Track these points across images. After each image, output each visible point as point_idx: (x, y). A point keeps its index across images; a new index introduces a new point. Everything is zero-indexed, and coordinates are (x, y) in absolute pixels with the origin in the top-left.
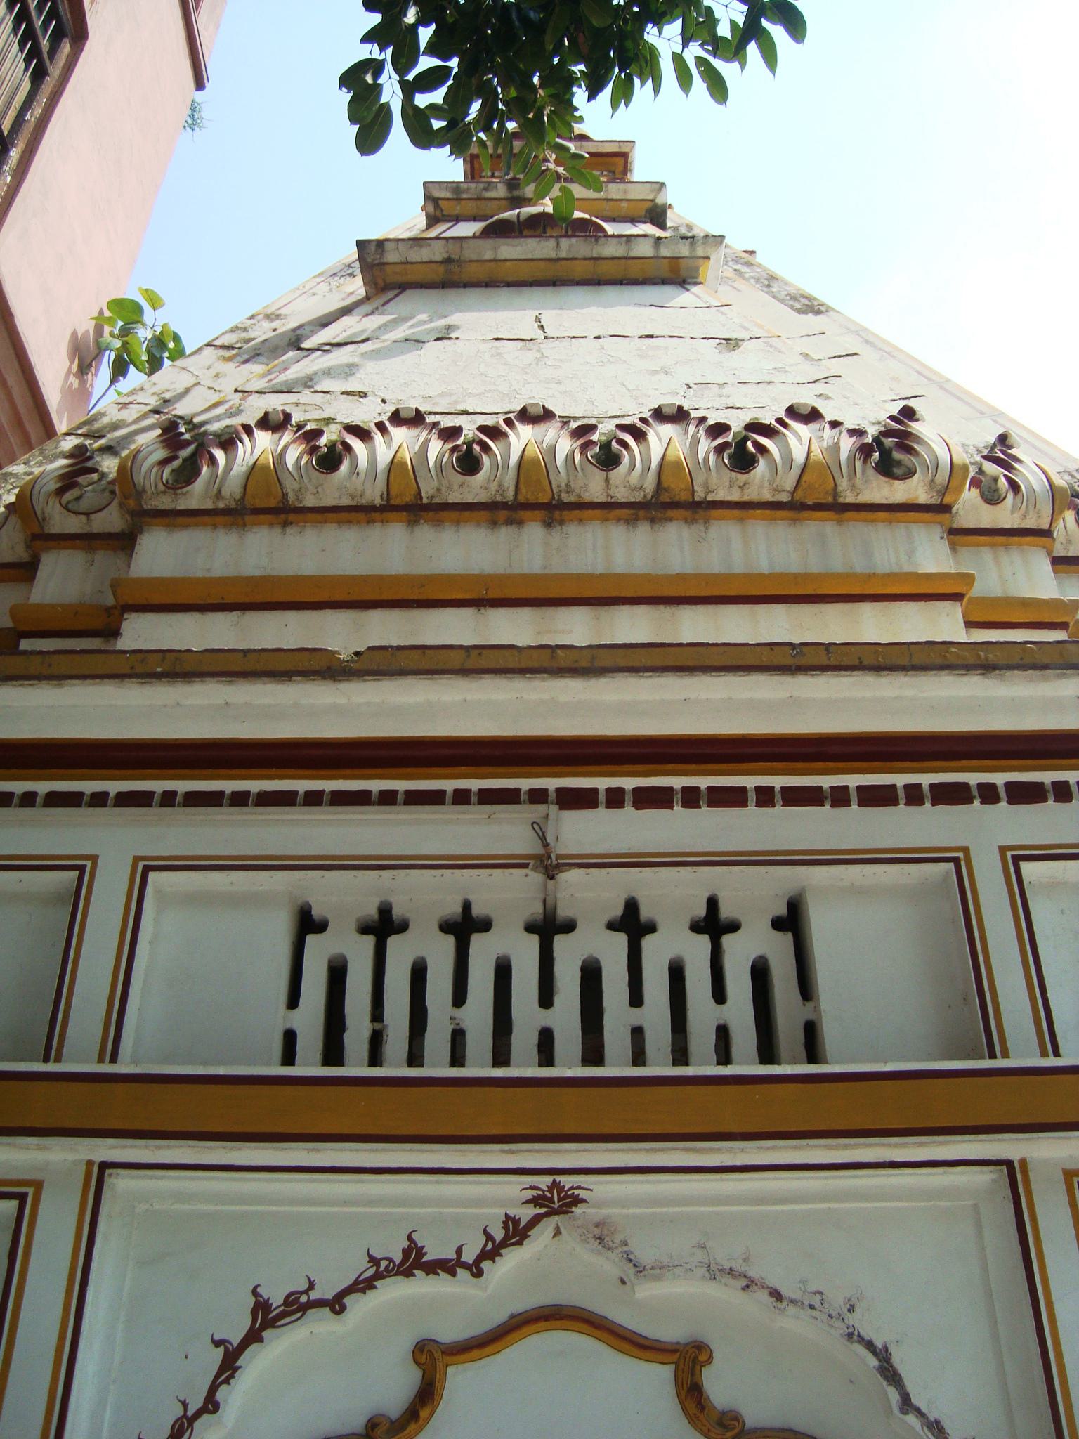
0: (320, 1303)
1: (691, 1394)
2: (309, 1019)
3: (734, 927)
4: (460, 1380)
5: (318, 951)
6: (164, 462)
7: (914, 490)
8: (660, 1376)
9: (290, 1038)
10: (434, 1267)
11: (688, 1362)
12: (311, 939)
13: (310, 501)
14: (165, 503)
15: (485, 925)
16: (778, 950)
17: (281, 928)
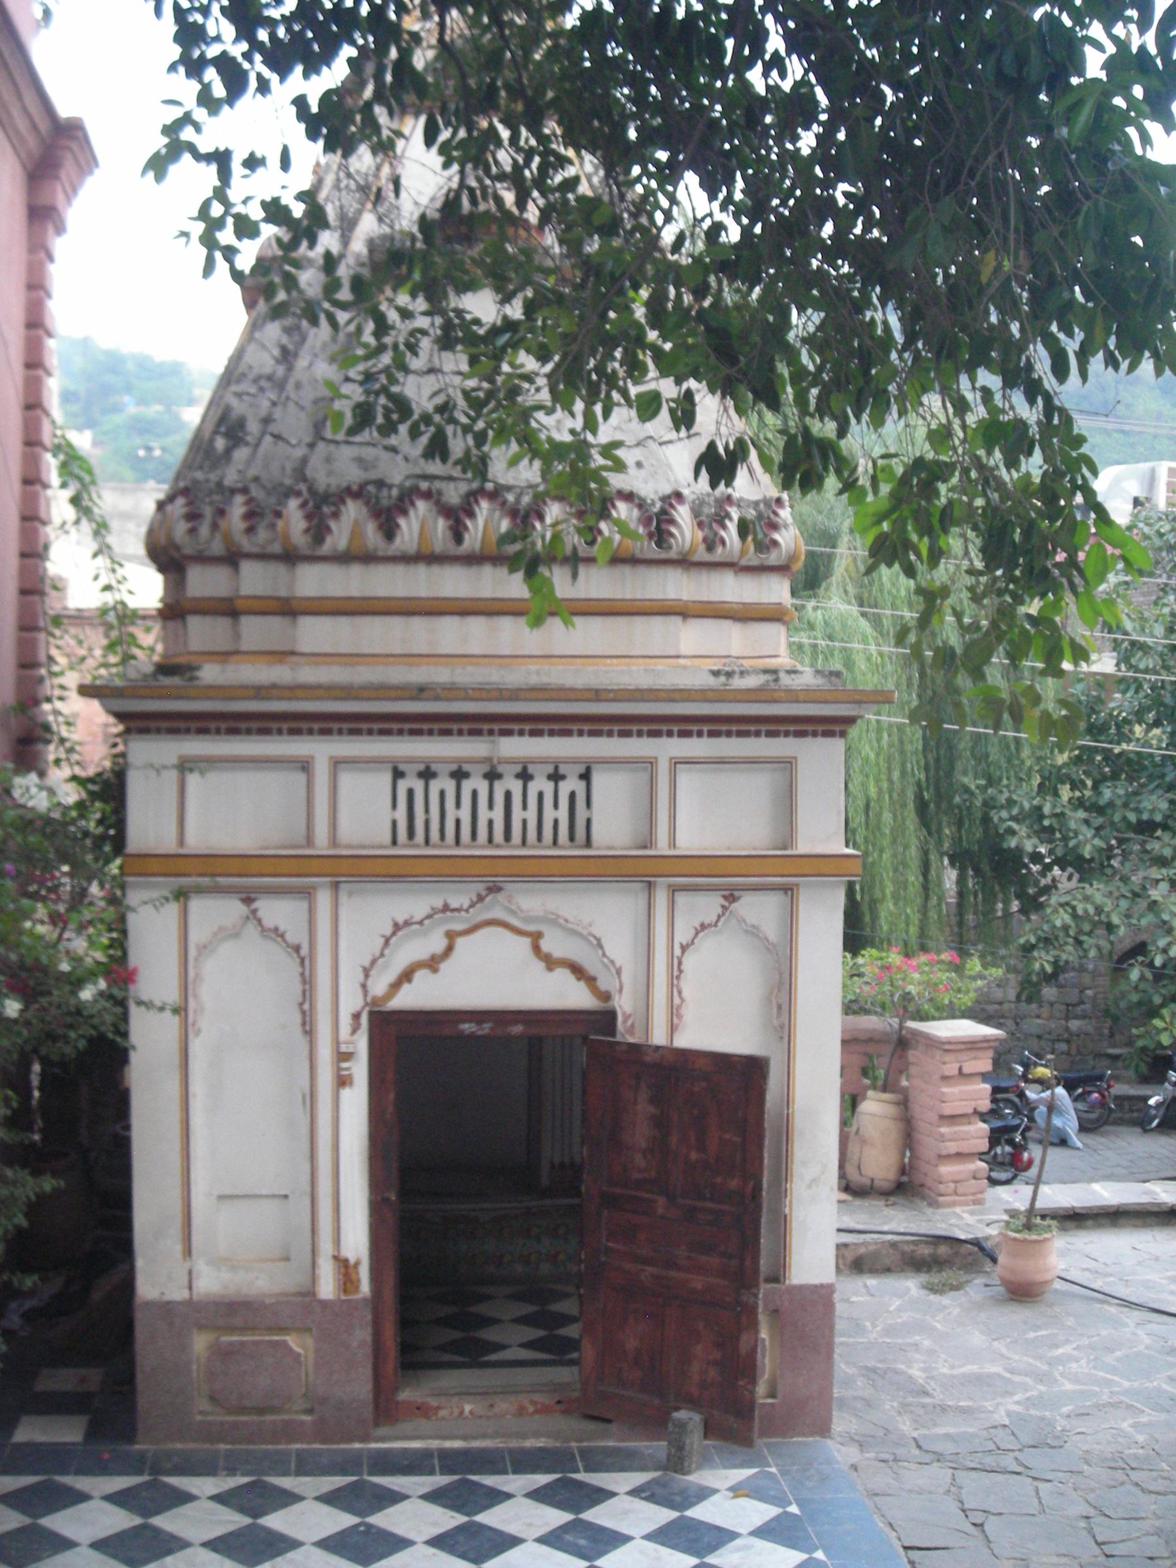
1: (536, 949)
3: (563, 777)
4: (460, 942)
5: (403, 786)
6: (307, 531)
7: (673, 554)
8: (527, 941)
9: (394, 824)
10: (454, 910)
11: (536, 937)
13: (380, 553)
14: (307, 552)
15: (466, 775)
16: (579, 787)
17: (387, 778)
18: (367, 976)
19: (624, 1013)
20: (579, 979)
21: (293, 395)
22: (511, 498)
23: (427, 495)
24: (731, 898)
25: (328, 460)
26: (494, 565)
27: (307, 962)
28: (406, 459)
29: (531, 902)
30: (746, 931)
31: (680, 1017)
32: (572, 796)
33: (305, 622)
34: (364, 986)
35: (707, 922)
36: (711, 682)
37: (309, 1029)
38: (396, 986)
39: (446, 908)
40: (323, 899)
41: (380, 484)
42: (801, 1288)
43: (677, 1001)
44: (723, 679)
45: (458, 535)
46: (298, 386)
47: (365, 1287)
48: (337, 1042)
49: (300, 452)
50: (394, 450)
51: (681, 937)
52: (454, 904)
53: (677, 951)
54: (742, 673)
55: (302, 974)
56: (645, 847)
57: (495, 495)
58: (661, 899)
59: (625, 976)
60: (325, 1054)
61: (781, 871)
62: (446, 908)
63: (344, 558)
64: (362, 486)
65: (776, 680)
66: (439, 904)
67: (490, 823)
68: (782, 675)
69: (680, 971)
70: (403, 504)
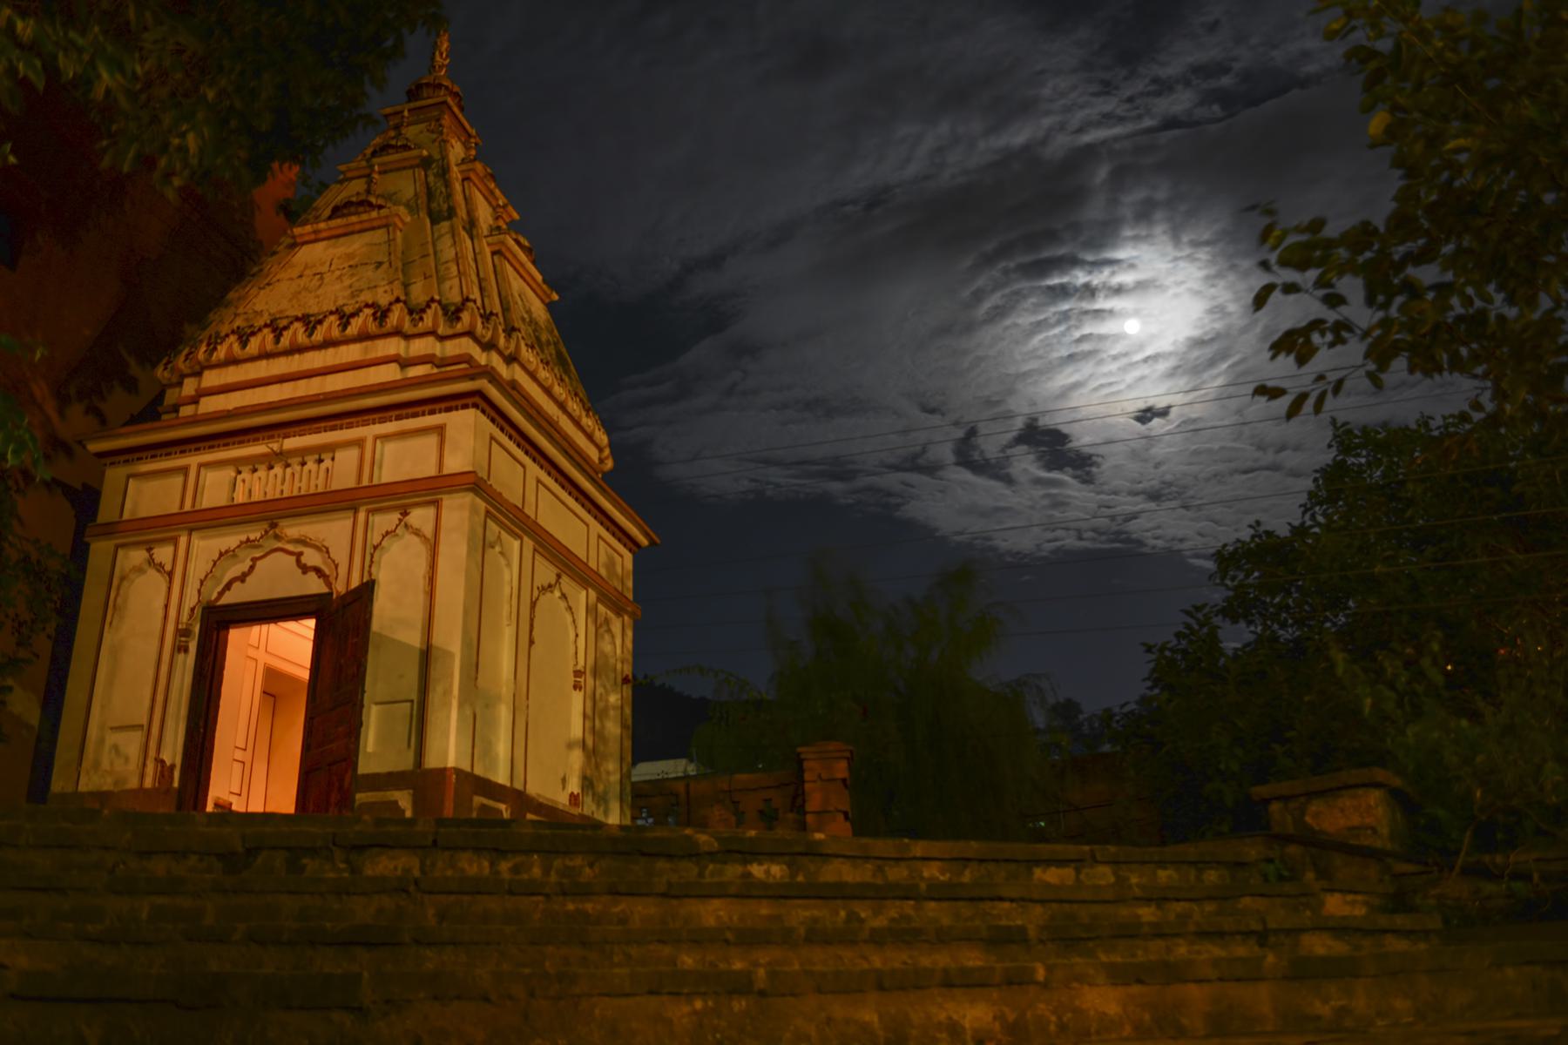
1: (298, 561)
4: (259, 563)
24: (405, 514)
29: (292, 529)
33: (204, 400)
38: (221, 594)
39: (248, 540)
40: (183, 540)
42: (432, 771)
47: (176, 784)
48: (177, 623)
51: (375, 538)
52: (252, 537)
62: (248, 540)
66: (244, 538)
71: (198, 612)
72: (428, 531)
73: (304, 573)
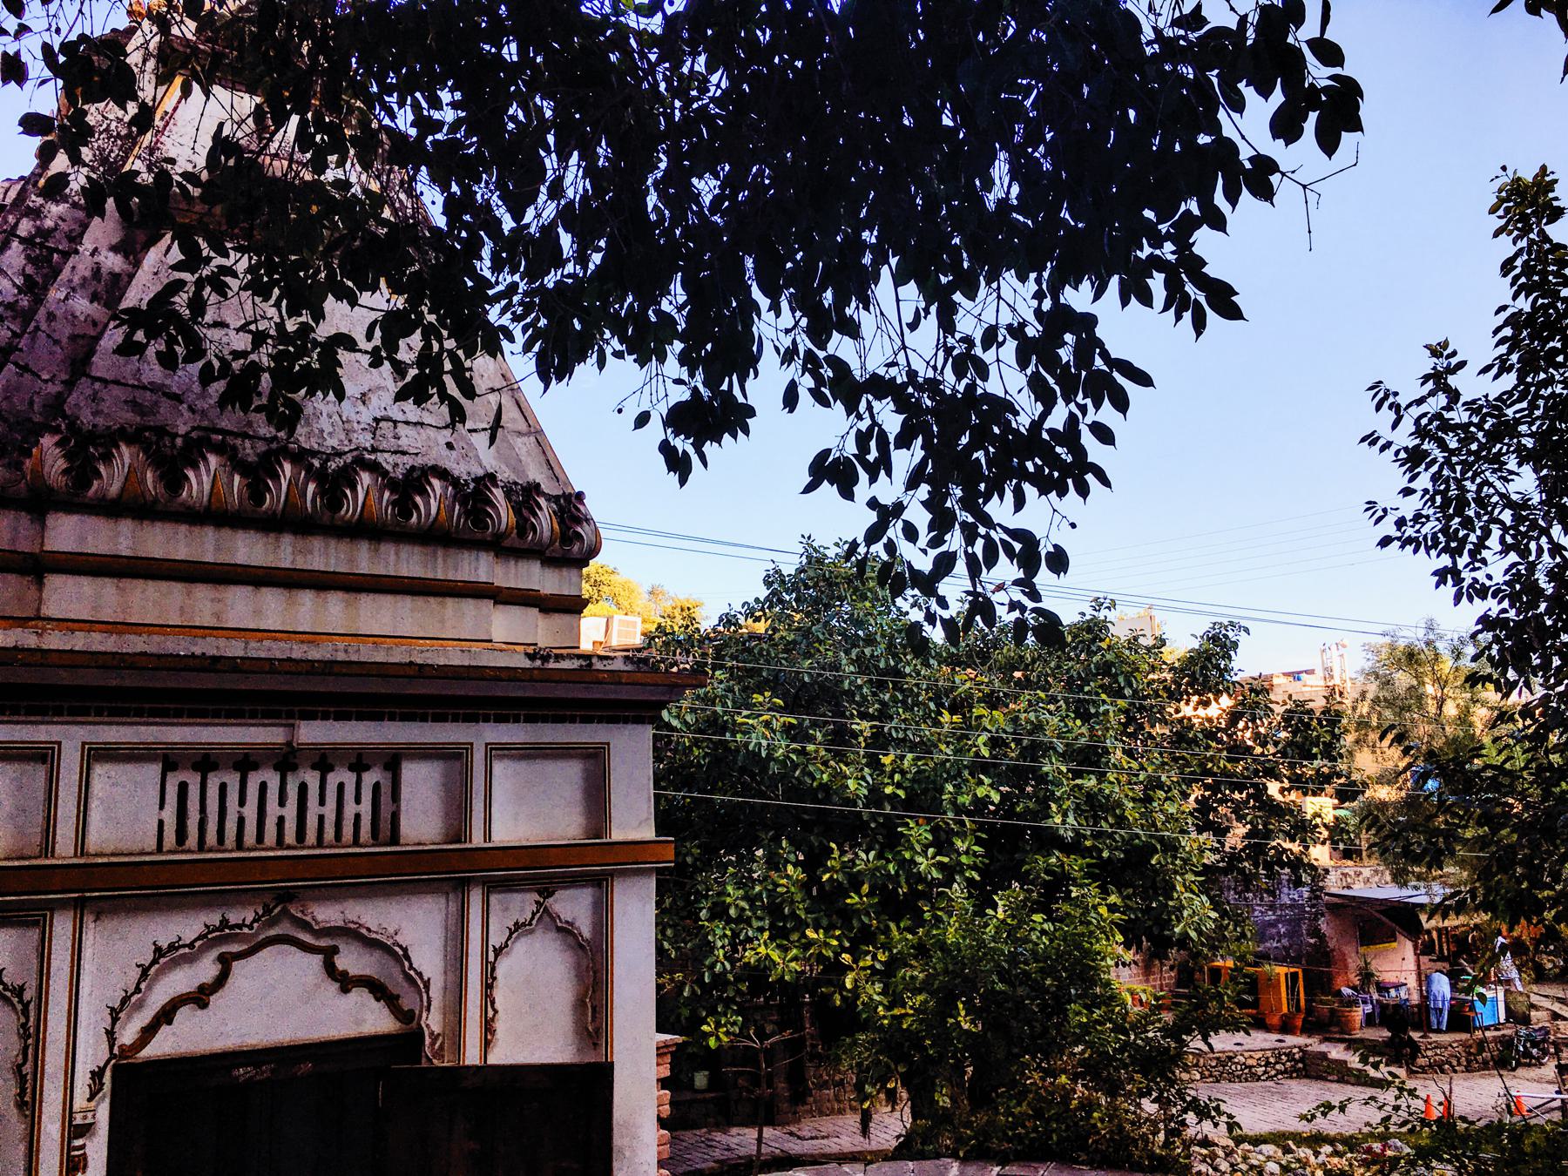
0: (184, 946)
2: (169, 816)
8: (316, 960)
9: (161, 823)
11: (329, 954)
12: (170, 775)
13: (159, 507)
17: (155, 770)
18: (115, 1020)
19: (432, 1033)
20: (378, 1000)
21: (44, 326)
22: (316, 463)
23: (219, 449)
24: (547, 893)
25: (95, 398)
26: (295, 533)
27: (32, 1006)
28: (191, 409)
30: (559, 930)
31: (493, 1032)
32: (377, 787)
34: (110, 1034)
35: (521, 921)
36: (527, 664)
37: (29, 1104)
38: (149, 1032)
39: (224, 923)
41: (161, 431)
43: (490, 1013)
44: (538, 663)
45: (256, 491)
46: (51, 317)
49: (53, 389)
50: (177, 398)
51: (496, 940)
53: (491, 958)
54: (558, 658)
55: (24, 1026)
56: (459, 842)
57: (301, 457)
58: (476, 897)
59: (436, 992)
60: (51, 1129)
61: (592, 864)
62: (224, 923)
63: (112, 509)
64: (142, 428)
65: (591, 664)
67: (281, 820)
68: (594, 660)
69: (494, 979)
70: (193, 452)
71: (107, 1078)
72: (586, 931)
73: (345, 990)
